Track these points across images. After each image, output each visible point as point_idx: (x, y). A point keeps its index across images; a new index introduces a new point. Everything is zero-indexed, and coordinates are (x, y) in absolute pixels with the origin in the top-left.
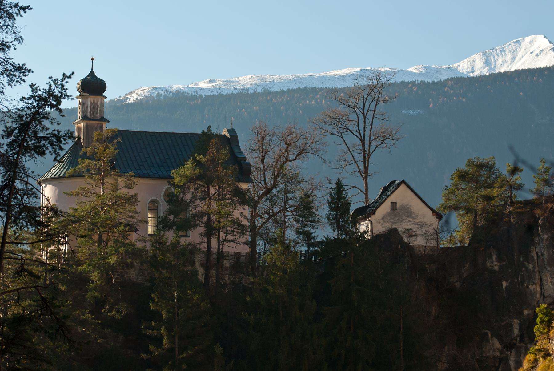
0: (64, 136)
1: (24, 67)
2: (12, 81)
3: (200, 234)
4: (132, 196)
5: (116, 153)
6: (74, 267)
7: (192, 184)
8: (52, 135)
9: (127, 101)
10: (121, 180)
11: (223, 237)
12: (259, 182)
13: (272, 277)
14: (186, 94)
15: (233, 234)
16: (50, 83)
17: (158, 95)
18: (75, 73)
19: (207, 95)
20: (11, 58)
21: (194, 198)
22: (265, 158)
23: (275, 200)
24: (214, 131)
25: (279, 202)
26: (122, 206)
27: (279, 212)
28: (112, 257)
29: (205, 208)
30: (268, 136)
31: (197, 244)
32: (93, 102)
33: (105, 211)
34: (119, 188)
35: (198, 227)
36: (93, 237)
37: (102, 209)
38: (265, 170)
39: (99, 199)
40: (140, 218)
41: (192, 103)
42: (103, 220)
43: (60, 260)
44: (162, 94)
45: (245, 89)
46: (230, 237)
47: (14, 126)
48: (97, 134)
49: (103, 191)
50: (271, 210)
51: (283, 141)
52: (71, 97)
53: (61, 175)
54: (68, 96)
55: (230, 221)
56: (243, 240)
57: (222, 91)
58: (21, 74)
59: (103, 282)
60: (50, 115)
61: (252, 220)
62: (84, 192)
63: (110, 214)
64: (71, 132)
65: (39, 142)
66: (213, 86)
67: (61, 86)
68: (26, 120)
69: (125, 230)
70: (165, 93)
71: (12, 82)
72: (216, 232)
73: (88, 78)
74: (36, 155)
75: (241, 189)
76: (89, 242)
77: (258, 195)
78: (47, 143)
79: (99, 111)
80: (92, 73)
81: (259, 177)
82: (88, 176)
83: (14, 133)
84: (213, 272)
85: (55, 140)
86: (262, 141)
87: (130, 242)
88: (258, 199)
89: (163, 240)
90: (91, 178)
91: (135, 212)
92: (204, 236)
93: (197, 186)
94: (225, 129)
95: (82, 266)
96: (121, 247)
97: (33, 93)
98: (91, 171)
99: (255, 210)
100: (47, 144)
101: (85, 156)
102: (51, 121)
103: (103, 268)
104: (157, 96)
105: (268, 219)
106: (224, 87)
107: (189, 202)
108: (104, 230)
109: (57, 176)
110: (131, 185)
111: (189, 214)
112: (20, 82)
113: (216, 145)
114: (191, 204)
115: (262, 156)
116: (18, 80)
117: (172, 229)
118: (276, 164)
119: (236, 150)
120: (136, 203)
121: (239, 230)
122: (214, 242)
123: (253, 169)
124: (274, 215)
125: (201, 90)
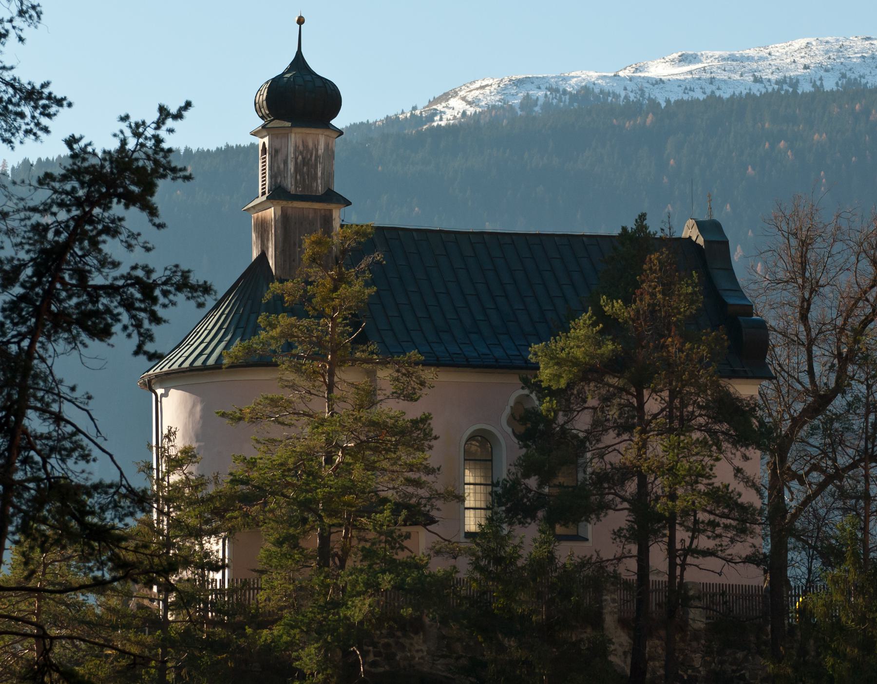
0: (165, 283)
1: (46, 91)
2: (13, 131)
3: (614, 533)
4: (415, 422)
5: (370, 296)
6: (249, 630)
7: (592, 384)
8: (129, 282)
9: (433, 121)
10: (385, 375)
11: (683, 541)
12: (791, 376)
13: (829, 661)
14: (610, 99)
15: (713, 532)
16: (122, 132)
17: (528, 103)
18: (193, 103)
19: (672, 100)
20: (8, 65)
21: (599, 427)
22: (812, 306)
23: (836, 430)
24: (654, 227)
25: (848, 436)
26: (388, 450)
27: (853, 466)
28: (357, 601)
29: (631, 455)
30: (819, 240)
31: (608, 560)
32: (301, 148)
33: (337, 467)
34: (379, 398)
35: (610, 512)
36: (302, 543)
37: (329, 460)
38: (811, 342)
39: (320, 430)
40: (440, 487)
41: (627, 125)
42: (330, 493)
43: (205, 610)
44: (537, 98)
45: (788, 80)
46: (704, 542)
47: (23, 255)
48: (313, 242)
49: (331, 408)
50: (830, 459)
51: (864, 255)
52: (182, 174)
53: (211, 361)
54: (174, 170)
55: (705, 494)
56: (742, 549)
57: (719, 89)
58: (38, 111)
59: (332, 676)
60: (123, 223)
61: (776, 487)
62: (276, 409)
63: (351, 474)
64: (183, 272)
65: (94, 300)
66: (691, 72)
67: (153, 141)
68: (56, 238)
69: (396, 523)
70: (546, 95)
71: (13, 134)
72: (664, 527)
73: (288, 75)
74: (84, 337)
75: (737, 398)
76: (292, 556)
77: (791, 415)
78: (115, 303)
79: (319, 174)
80: (299, 62)
81: (794, 360)
82: (287, 364)
83: (23, 277)
84: (654, 646)
85: (138, 296)
86: (801, 257)
87: (410, 557)
88: (792, 429)
89: (508, 549)
90: (298, 370)
91: (426, 467)
92: (627, 539)
93: (608, 391)
94: (690, 222)
95: (271, 629)
96: (383, 572)
97: (74, 164)
98: (297, 347)
99: (783, 460)
100: (116, 307)
101: (277, 306)
102: (126, 242)
103: (332, 635)
104: (522, 106)
105: (822, 486)
106: (723, 76)
107: (585, 437)
108: (335, 521)
109: (199, 363)
110: (414, 389)
111: (585, 472)
112: (35, 134)
113: (660, 269)
114: (591, 444)
115: (803, 300)
116: (28, 127)
117: (534, 518)
118: (845, 324)
119: (722, 284)
120: (426, 443)
121: (733, 519)
122: (658, 557)
123: (774, 338)
124: (839, 474)
125: (653, 85)
